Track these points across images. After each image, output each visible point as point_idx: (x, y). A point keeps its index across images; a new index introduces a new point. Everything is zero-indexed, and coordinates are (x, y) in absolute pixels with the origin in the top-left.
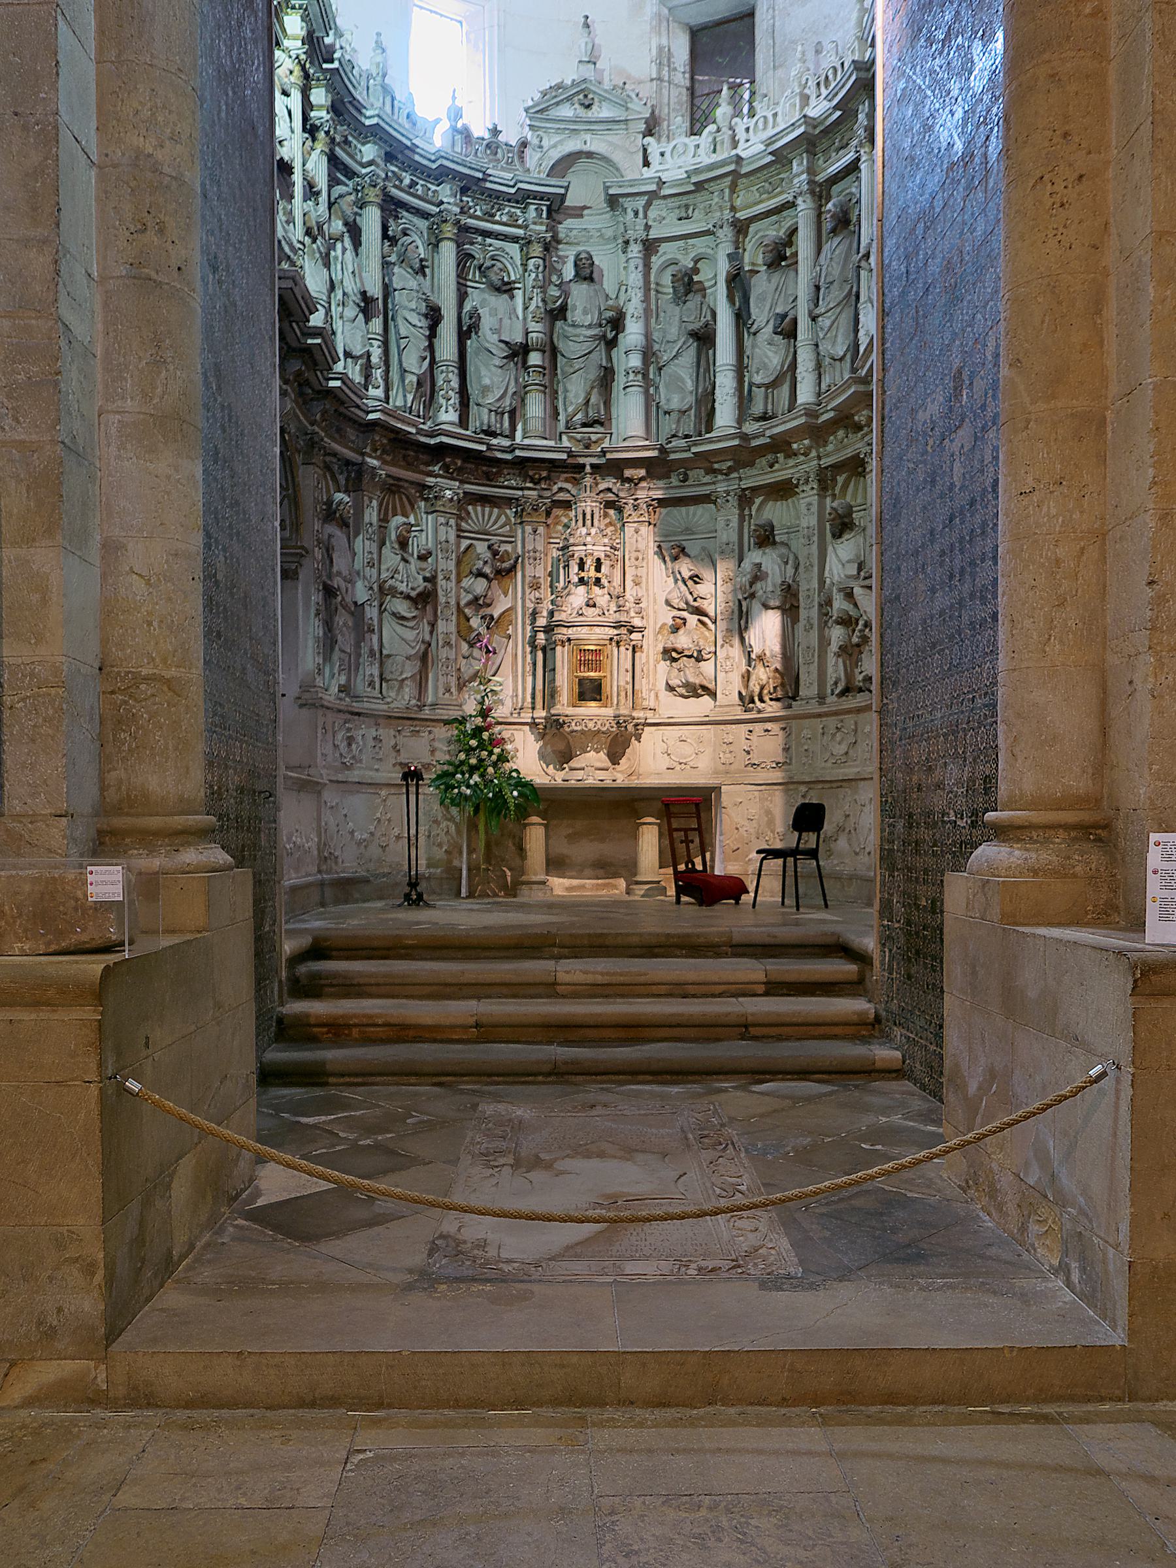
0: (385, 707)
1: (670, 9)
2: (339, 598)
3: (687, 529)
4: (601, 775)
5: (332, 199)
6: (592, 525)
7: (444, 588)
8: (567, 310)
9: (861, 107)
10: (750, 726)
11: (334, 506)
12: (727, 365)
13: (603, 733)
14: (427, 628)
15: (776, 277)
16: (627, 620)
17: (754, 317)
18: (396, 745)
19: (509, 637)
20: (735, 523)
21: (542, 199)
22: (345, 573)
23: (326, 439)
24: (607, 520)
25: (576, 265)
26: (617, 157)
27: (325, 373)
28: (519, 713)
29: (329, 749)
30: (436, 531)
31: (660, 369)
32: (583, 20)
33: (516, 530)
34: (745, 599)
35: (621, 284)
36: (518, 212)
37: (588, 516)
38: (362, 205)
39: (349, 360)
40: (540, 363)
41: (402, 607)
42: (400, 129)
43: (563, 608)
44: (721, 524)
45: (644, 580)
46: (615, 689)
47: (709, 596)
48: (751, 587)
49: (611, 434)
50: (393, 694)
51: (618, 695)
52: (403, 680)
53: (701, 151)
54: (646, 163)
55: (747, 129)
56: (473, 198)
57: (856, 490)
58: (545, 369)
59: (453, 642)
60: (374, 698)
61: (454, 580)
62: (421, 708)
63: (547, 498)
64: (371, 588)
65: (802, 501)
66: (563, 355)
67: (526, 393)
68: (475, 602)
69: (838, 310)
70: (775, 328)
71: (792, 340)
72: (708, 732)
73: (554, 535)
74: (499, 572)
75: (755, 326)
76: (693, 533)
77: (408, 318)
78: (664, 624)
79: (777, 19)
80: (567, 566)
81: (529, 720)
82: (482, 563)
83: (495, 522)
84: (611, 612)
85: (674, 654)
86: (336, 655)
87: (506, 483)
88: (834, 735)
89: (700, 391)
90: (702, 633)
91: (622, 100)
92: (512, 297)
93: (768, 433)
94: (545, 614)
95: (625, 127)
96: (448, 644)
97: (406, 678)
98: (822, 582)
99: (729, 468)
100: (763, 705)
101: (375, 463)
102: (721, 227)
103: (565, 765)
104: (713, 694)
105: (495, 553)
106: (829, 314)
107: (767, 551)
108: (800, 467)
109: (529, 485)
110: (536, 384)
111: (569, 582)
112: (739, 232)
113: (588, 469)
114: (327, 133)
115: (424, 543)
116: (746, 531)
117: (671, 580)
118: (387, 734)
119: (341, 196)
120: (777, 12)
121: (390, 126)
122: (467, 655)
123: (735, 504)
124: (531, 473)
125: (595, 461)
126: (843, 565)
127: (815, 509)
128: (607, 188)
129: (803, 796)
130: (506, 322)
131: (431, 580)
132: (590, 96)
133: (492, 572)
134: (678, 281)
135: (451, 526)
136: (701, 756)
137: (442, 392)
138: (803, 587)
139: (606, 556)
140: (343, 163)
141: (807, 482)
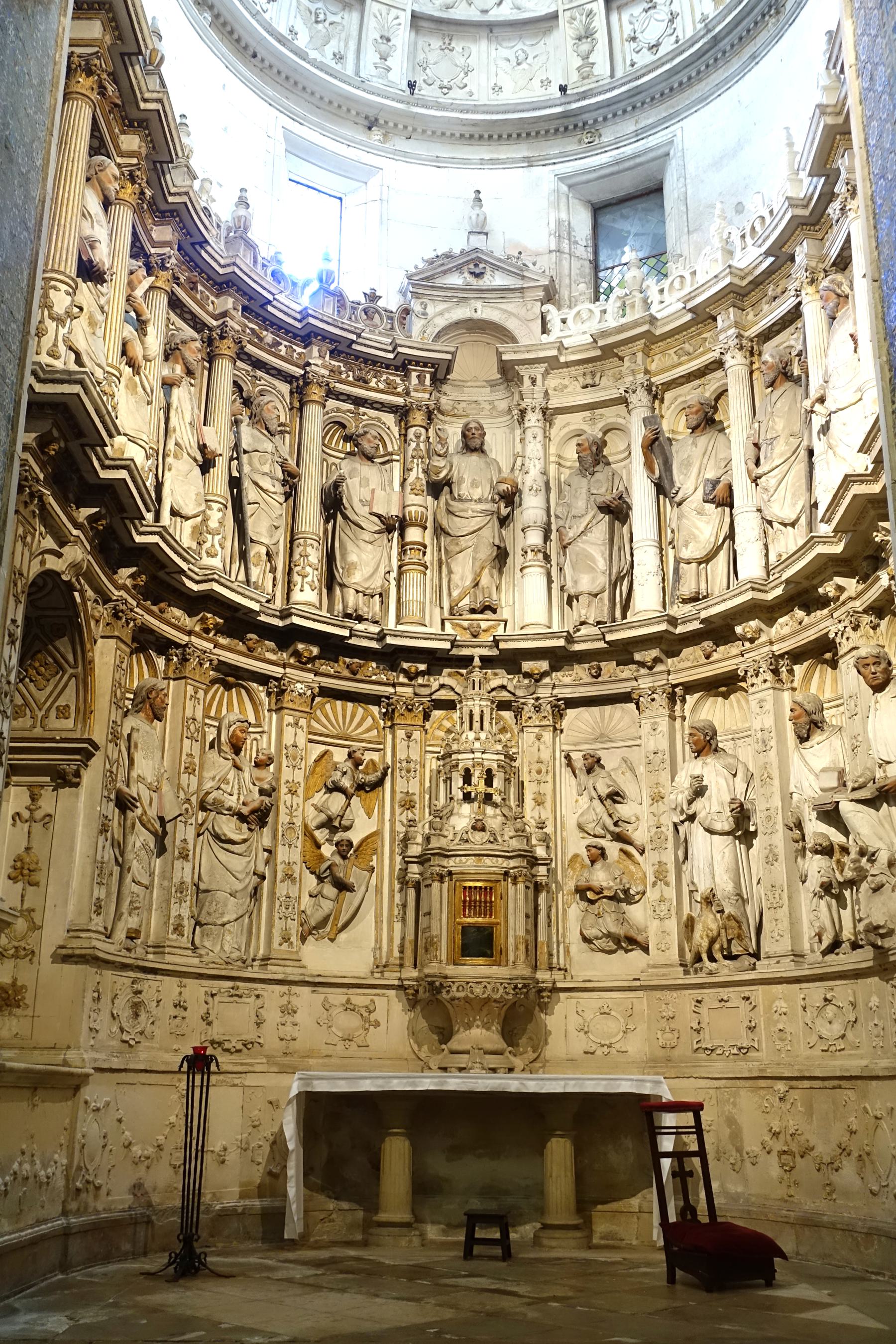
1: (570, 187)
2: (139, 811)
6: (482, 729)
7: (289, 804)
9: (798, 249)
10: (697, 994)
12: (647, 540)
13: (495, 1001)
15: (703, 440)
16: (527, 848)
17: (678, 485)
19: (372, 870)
20: (664, 724)
21: (425, 365)
25: (464, 435)
26: (511, 325)
28: (382, 972)
29: (103, 1021)
30: (280, 732)
31: (565, 547)
32: (474, 195)
33: (385, 738)
34: (682, 822)
35: (516, 456)
36: (398, 380)
37: (477, 718)
41: (229, 827)
46: (511, 940)
47: (633, 819)
49: (506, 622)
51: (516, 948)
52: (223, 925)
53: (608, 316)
54: (545, 330)
55: (662, 291)
57: (822, 682)
59: (296, 875)
61: (301, 795)
64: (188, 801)
65: (751, 698)
66: (448, 534)
68: (329, 824)
69: (785, 467)
70: (705, 494)
71: (727, 510)
72: (641, 1002)
74: (361, 787)
76: (611, 741)
77: (261, 484)
78: (576, 856)
79: (689, 187)
81: (396, 982)
82: (339, 774)
83: (359, 725)
84: (506, 838)
85: (590, 895)
87: (374, 678)
89: (614, 571)
93: (704, 615)
94: (419, 839)
96: (289, 876)
102: (634, 392)
103: (443, 1046)
104: (646, 950)
105: (357, 763)
107: (710, 759)
110: (414, 564)
111: (451, 799)
112: (655, 397)
113: (477, 662)
115: (265, 746)
117: (584, 801)
120: (688, 181)
121: (250, 277)
123: (664, 704)
124: (405, 665)
125: (485, 652)
126: (816, 775)
127: (769, 706)
128: (499, 354)
129: (780, 1099)
130: (379, 493)
132: (481, 266)
133: (351, 787)
134: (584, 450)
136: (630, 1035)
140: (191, 313)
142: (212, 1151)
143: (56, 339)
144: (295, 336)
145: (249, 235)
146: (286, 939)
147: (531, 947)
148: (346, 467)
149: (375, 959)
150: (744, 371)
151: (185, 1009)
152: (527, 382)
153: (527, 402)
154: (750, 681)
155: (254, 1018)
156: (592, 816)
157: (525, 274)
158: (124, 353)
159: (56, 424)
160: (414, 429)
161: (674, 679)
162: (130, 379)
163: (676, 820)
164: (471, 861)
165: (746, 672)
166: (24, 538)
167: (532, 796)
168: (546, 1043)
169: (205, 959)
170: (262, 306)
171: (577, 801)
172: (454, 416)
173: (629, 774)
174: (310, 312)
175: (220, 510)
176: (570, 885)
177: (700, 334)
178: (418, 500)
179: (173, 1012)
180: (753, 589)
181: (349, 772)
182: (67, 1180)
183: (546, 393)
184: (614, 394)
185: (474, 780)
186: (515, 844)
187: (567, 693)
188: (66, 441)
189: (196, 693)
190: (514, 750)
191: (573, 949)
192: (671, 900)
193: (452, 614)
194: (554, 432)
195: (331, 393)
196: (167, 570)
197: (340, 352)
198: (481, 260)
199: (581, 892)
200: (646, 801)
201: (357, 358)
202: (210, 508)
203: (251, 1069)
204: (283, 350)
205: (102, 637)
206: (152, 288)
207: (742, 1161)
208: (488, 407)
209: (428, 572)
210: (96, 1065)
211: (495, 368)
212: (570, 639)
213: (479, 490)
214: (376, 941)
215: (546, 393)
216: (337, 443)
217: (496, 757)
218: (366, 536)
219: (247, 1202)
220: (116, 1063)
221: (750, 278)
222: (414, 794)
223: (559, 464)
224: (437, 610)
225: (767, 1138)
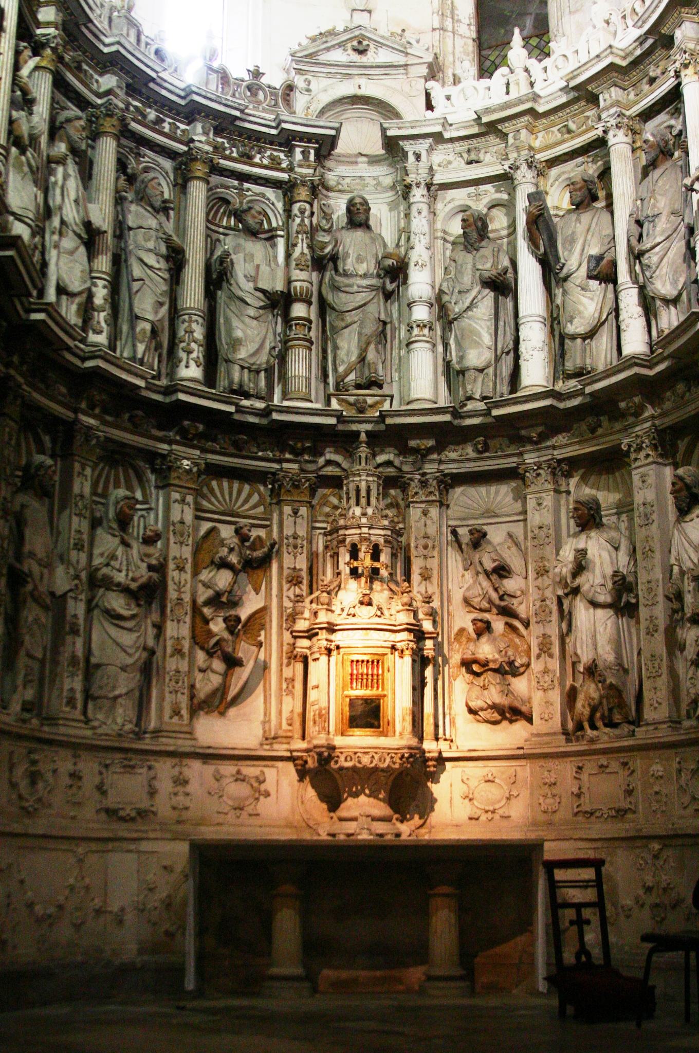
0: (89, 733)
2: (30, 587)
4: (380, 828)
5: (58, 124)
6: (368, 504)
8: (338, 258)
11: (32, 471)
13: (383, 770)
14: (151, 632)
16: (414, 622)
17: (563, 261)
18: (102, 783)
19: (260, 645)
21: (309, 141)
22: (40, 552)
23: (25, 387)
25: (349, 210)
27: (24, 299)
30: (167, 509)
31: (450, 323)
33: (271, 515)
34: (567, 595)
36: (282, 156)
37: (363, 493)
38: (95, 136)
39: (64, 297)
41: (117, 603)
42: (145, 60)
44: (531, 503)
47: (518, 593)
49: (392, 397)
50: (100, 716)
52: (116, 698)
54: (430, 107)
55: (545, 69)
56: (230, 140)
58: (310, 322)
59: (186, 649)
60: (73, 720)
62: (139, 735)
64: (77, 577)
66: (333, 309)
67: (287, 349)
68: (216, 601)
71: (611, 286)
73: (319, 518)
75: (565, 271)
76: (497, 516)
78: (462, 631)
80: (335, 556)
82: (226, 550)
83: (246, 501)
84: (393, 611)
85: (475, 668)
86: (22, 661)
87: (260, 454)
90: (512, 640)
91: (401, 45)
92: (274, 246)
93: (588, 390)
95: (404, 72)
96: (178, 651)
97: (120, 696)
100: (595, 732)
101: (92, 422)
103: (332, 814)
104: (530, 720)
106: (657, 249)
107: (593, 534)
109: (288, 456)
113: (363, 437)
114: (54, 50)
115: (152, 522)
117: (468, 575)
119: (68, 121)
121: (133, 55)
122: (204, 666)
123: (549, 478)
125: (369, 427)
128: (384, 130)
130: (264, 269)
131: (160, 569)
132: (365, 43)
133: (239, 562)
134: (469, 226)
135: (188, 504)
136: (513, 801)
137: (183, 345)
138: (643, 578)
139: (385, 542)
141: (639, 449)
142: (111, 912)
145: (133, 14)
146: (176, 712)
148: (229, 243)
149: (265, 732)
150: (627, 150)
152: (411, 158)
153: (411, 178)
154: (633, 456)
155: (146, 788)
156: (477, 590)
157: (409, 51)
158: (10, 132)
160: (298, 205)
161: (559, 454)
162: (16, 158)
163: (560, 592)
168: (432, 810)
169: (100, 731)
170: (146, 85)
171: (463, 576)
172: (339, 191)
173: (514, 549)
174: (194, 89)
175: (105, 287)
176: (456, 659)
177: (583, 112)
178: (303, 275)
179: (69, 782)
181: (237, 548)
183: (431, 169)
184: (498, 170)
185: (361, 555)
187: (452, 468)
189: (83, 469)
190: (401, 526)
192: (555, 671)
193: (337, 388)
194: (439, 206)
197: (223, 130)
198: (364, 37)
199: (467, 664)
200: (532, 575)
202: (95, 285)
203: (144, 835)
204: (167, 128)
206: (37, 68)
207: (617, 914)
209: (313, 347)
212: (456, 413)
213: (365, 265)
214: (265, 714)
218: (252, 312)
219: (145, 958)
222: (301, 570)
223: (445, 240)
225: (641, 892)
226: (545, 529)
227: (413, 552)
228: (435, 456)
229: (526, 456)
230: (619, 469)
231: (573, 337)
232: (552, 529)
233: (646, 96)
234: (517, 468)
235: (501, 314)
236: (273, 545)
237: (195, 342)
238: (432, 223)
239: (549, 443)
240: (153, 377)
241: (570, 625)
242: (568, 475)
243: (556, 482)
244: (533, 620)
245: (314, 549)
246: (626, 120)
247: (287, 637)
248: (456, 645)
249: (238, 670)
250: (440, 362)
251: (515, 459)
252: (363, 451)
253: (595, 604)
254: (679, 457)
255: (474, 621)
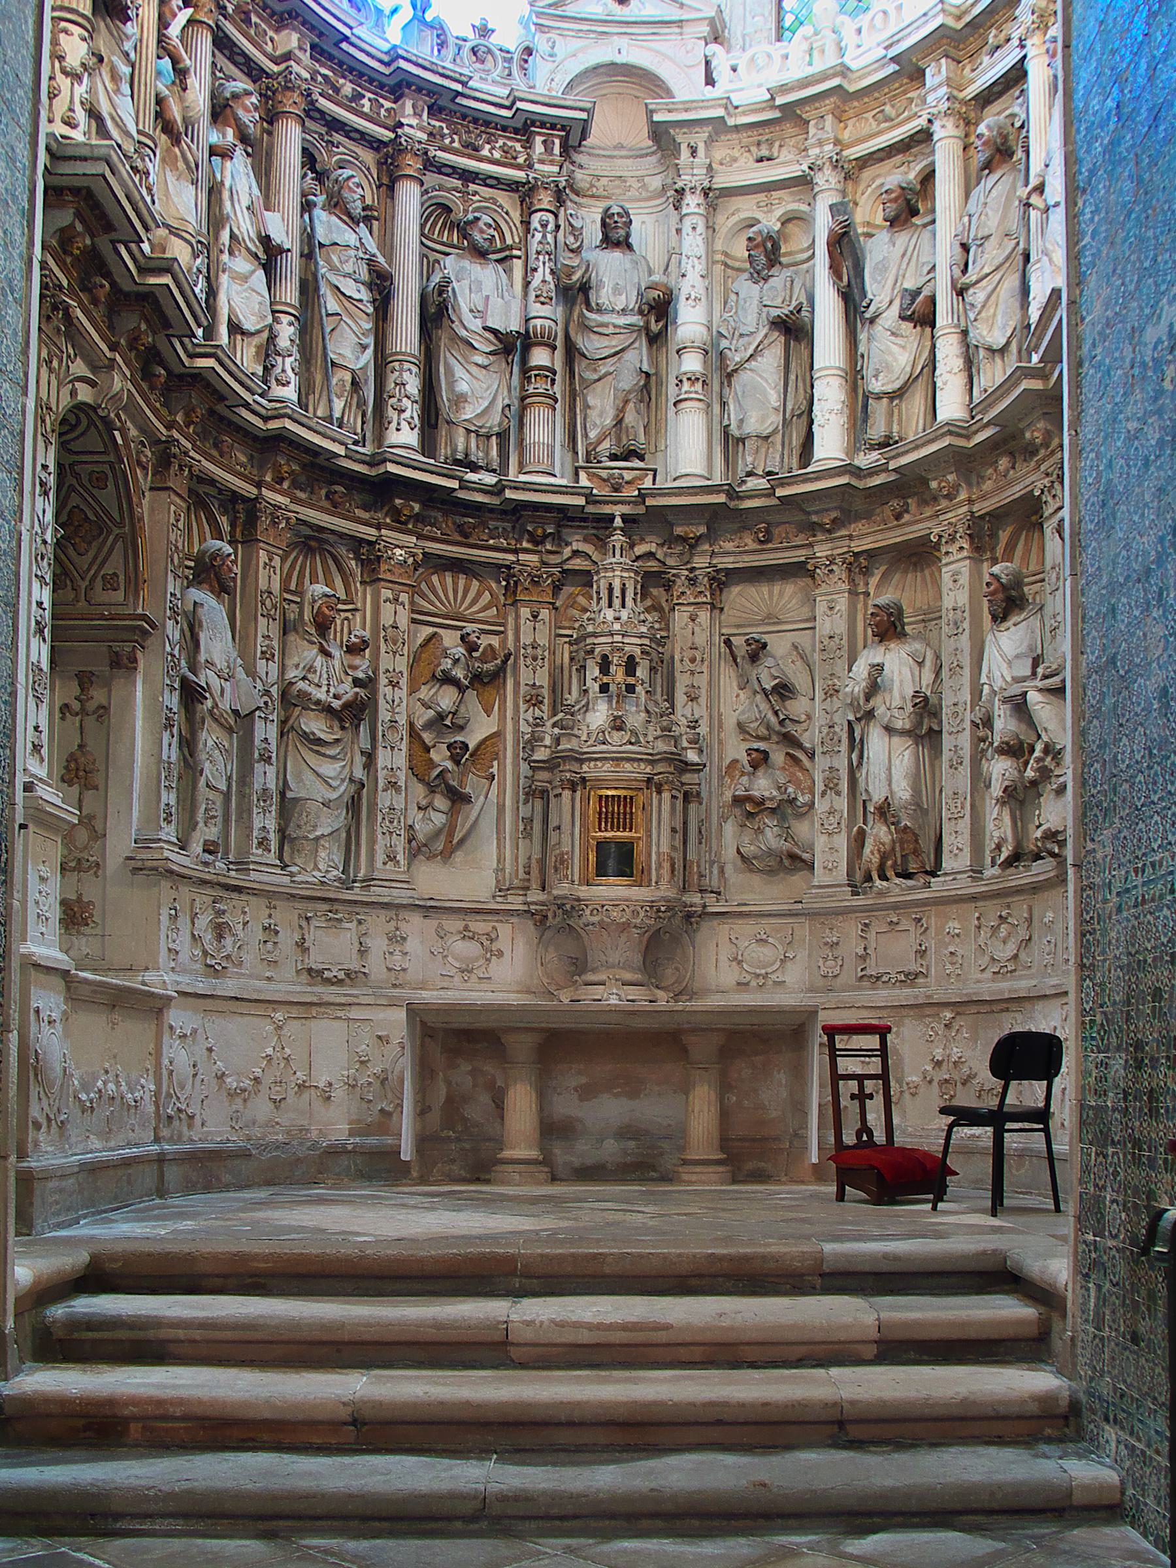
3: (769, 616)
7: (389, 699)
14: (359, 760)
17: (870, 296)
20: (842, 603)
21: (553, 127)
24: (649, 602)
25: (604, 224)
31: (729, 376)
33: (505, 618)
34: (859, 720)
36: (518, 147)
37: (617, 592)
40: (549, 365)
43: (576, 732)
44: (821, 607)
45: (703, 692)
47: (803, 717)
48: (867, 700)
49: (655, 471)
51: (659, 866)
52: (317, 839)
58: (554, 373)
59: (402, 783)
61: (405, 688)
63: (556, 566)
69: (998, 277)
70: (902, 309)
75: (872, 309)
76: (780, 623)
78: (736, 761)
82: (450, 661)
83: (474, 602)
84: (650, 738)
87: (491, 542)
88: (995, 929)
92: (509, 272)
94: (548, 741)
96: (393, 785)
98: (977, 692)
99: (834, 521)
105: (472, 648)
106: (984, 283)
107: (892, 646)
108: (941, 518)
109: (525, 545)
113: (618, 522)
116: (860, 617)
118: (286, 917)
122: (424, 803)
123: (843, 576)
125: (626, 509)
127: (964, 579)
129: (946, 1025)
130: (496, 302)
131: (368, 684)
134: (757, 246)
135: (403, 604)
141: (952, 539)
143: (72, 101)
144: (382, 86)
146: (392, 858)
147: (679, 865)
148: (451, 265)
150: (957, 146)
151: (277, 932)
154: (943, 550)
158: (158, 115)
159: (78, 215)
160: (539, 214)
161: (858, 546)
163: (851, 717)
164: (608, 766)
165: (940, 537)
166: (49, 362)
167: (684, 690)
170: (337, 45)
171: (738, 696)
172: (593, 196)
173: (799, 663)
174: (400, 52)
178: (545, 311)
180: (950, 433)
182: (157, 1104)
183: (710, 168)
185: (613, 669)
186: (661, 746)
187: (727, 562)
188: (92, 236)
190: (664, 634)
191: (729, 869)
192: (842, 811)
194: (720, 219)
195: (430, 164)
196: (228, 403)
197: (441, 110)
201: (464, 117)
205: (151, 489)
206: (190, 22)
208: (636, 185)
209: (558, 406)
210: (179, 988)
211: (645, 133)
215: (710, 168)
216: (441, 233)
217: (638, 641)
220: (201, 988)
221: (968, 18)
223: (726, 265)
224: (569, 456)
225: (929, 1068)
226: (836, 640)
227: (677, 664)
228: (706, 547)
229: (816, 549)
230: (929, 566)
231: (878, 397)
232: (845, 638)
233: (984, 72)
234: (805, 563)
235: (793, 365)
236: (507, 657)
237: (409, 398)
238: (709, 243)
239: (844, 532)
240: (356, 443)
241: (861, 757)
242: (866, 572)
243: (852, 581)
244: (818, 750)
245: (558, 662)
246: (957, 105)
247: (524, 767)
248: (727, 780)
249: (466, 808)
250: (716, 427)
251: (803, 552)
252: (618, 539)
253: (889, 730)
254: (999, 552)
255: (749, 751)
